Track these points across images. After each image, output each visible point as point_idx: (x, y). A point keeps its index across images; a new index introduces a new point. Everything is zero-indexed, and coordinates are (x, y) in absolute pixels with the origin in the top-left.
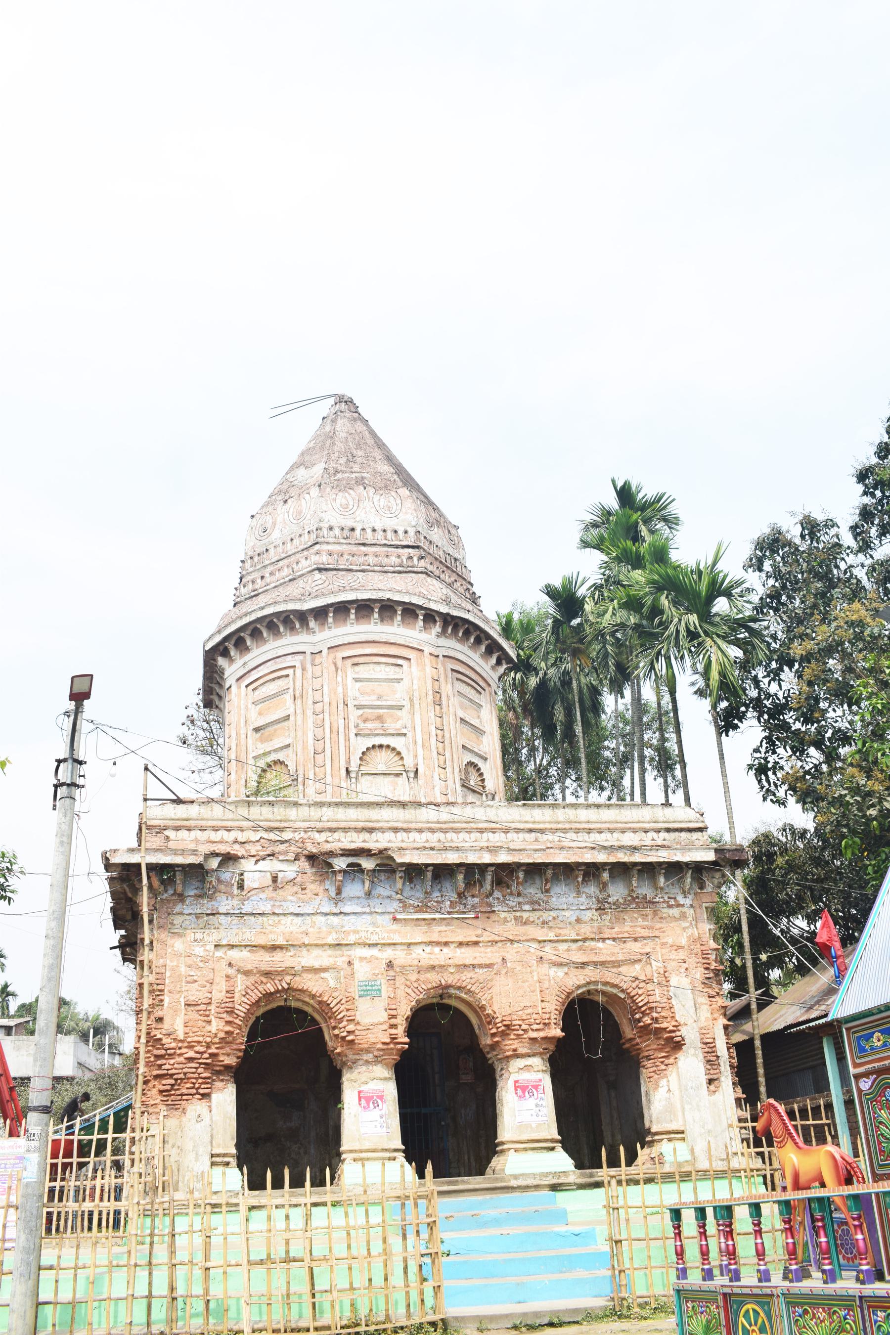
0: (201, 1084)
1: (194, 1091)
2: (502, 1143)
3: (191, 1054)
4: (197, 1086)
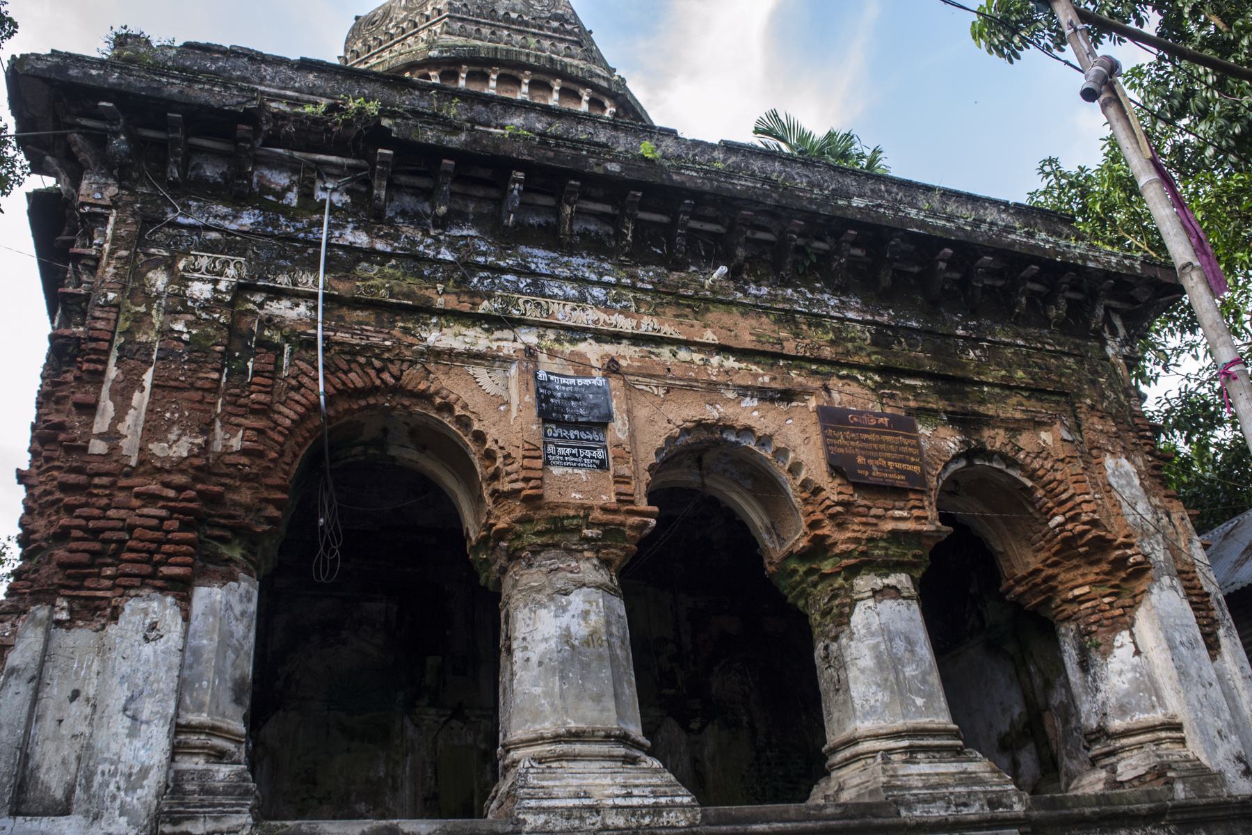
0: (170, 555)
1: (147, 569)
2: (834, 750)
3: (154, 487)
4: (157, 557)
